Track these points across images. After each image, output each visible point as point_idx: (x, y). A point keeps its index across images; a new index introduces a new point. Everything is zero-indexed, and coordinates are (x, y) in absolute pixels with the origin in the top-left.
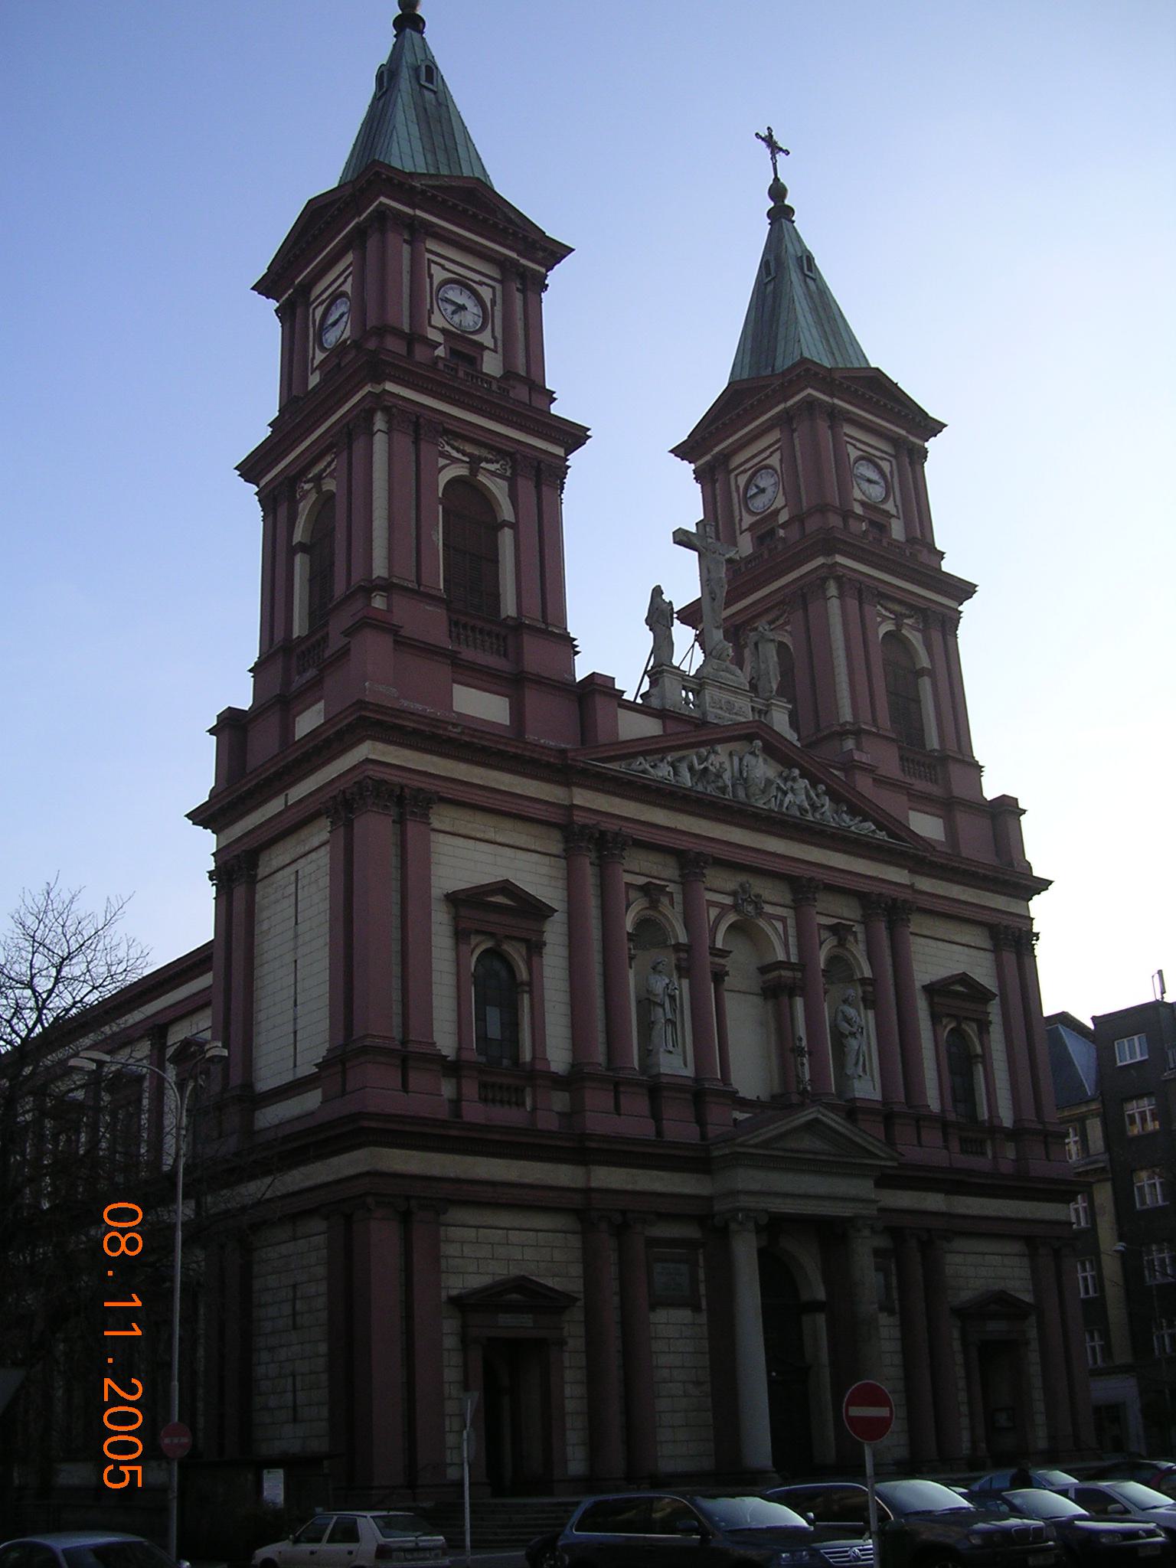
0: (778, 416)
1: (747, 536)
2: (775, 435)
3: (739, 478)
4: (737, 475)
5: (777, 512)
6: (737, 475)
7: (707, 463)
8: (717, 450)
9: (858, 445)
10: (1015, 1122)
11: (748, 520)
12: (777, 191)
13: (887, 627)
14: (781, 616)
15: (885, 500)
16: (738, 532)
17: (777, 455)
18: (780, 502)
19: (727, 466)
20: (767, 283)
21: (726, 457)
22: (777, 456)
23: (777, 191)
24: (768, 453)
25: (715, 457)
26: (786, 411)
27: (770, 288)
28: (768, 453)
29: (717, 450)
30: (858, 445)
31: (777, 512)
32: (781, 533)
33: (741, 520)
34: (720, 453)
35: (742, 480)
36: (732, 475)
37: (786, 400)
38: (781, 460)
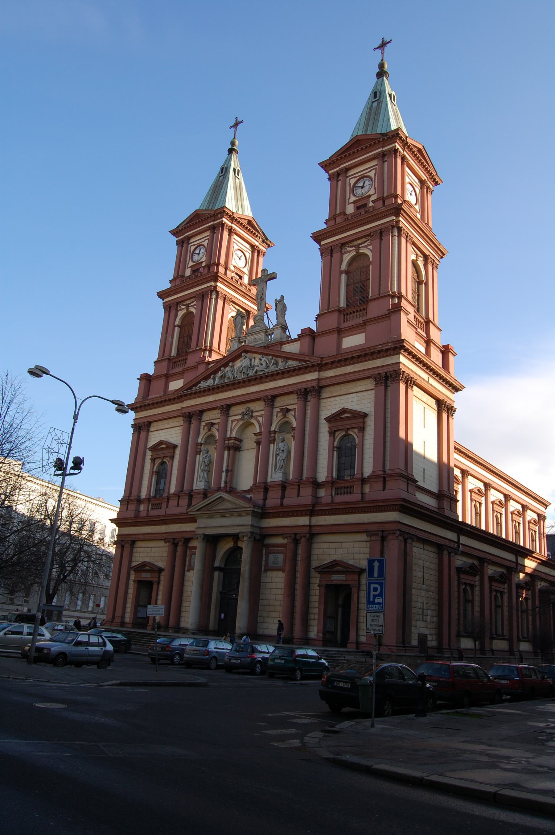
0: (378, 154)
1: (352, 205)
2: (375, 162)
3: (351, 180)
4: (350, 179)
5: (370, 196)
6: (350, 179)
7: (337, 172)
8: (342, 166)
9: (409, 177)
10: (439, 491)
11: (353, 199)
12: (381, 66)
13: (413, 257)
14: (366, 242)
15: (416, 204)
16: (347, 203)
17: (374, 172)
18: (372, 191)
19: (346, 174)
20: (373, 102)
21: (347, 169)
22: (374, 172)
23: (381, 66)
24: (369, 170)
25: (342, 169)
26: (383, 152)
27: (375, 104)
28: (369, 170)
29: (342, 166)
30: (409, 177)
31: (370, 196)
32: (371, 204)
33: (349, 198)
34: (345, 168)
35: (353, 181)
36: (348, 179)
37: (383, 147)
38: (375, 174)
